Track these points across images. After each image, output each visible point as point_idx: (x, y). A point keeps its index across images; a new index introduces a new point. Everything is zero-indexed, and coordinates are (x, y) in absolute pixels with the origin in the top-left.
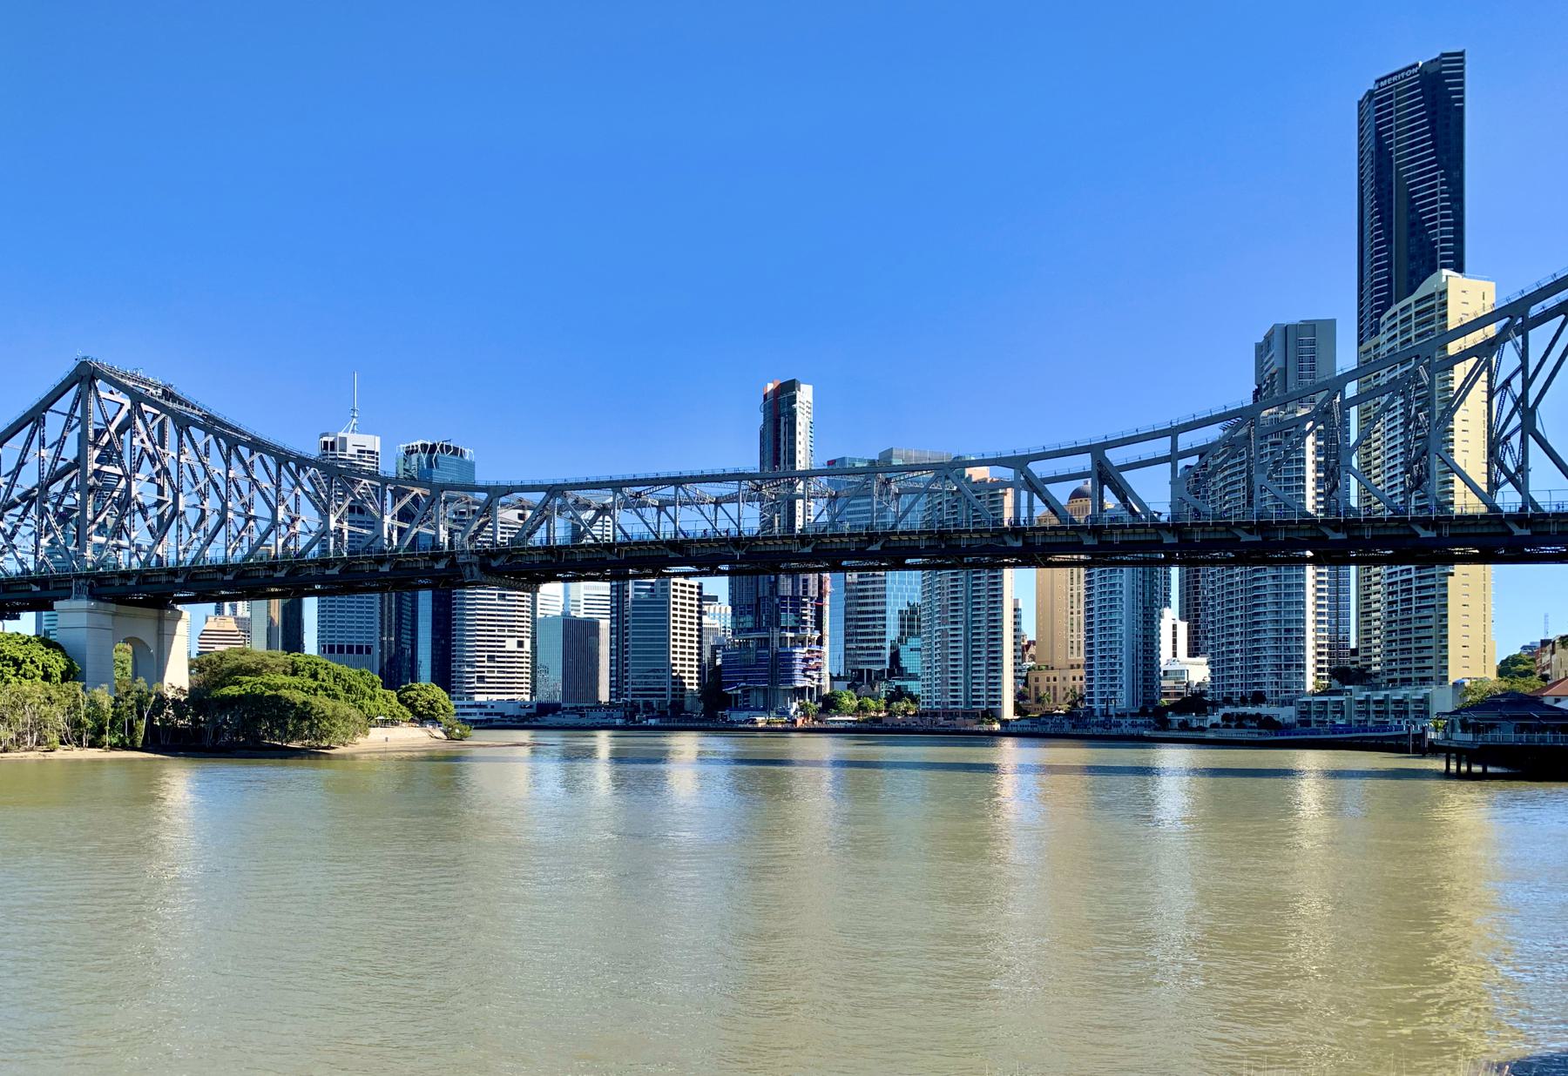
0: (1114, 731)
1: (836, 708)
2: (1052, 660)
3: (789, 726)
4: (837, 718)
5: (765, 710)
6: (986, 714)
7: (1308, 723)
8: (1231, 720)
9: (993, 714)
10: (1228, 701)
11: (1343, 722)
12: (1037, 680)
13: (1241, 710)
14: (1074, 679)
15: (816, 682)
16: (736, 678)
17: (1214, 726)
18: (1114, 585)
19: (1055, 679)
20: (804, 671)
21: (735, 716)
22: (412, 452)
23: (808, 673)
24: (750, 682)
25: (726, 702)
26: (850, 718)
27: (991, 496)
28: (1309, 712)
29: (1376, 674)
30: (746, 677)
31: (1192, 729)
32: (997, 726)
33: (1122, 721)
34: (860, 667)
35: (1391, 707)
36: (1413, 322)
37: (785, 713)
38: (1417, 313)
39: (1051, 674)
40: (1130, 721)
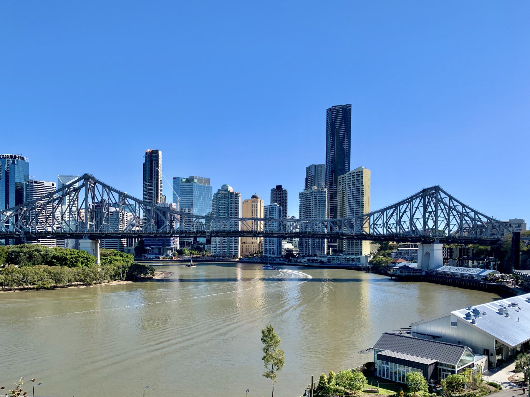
0: (274, 262)
1: (184, 254)
2: (247, 241)
3: (171, 259)
4: (185, 257)
5: (160, 254)
6: (234, 256)
7: (330, 262)
8: (310, 260)
9: (235, 256)
10: (308, 256)
11: (339, 262)
12: (243, 246)
13: (311, 258)
14: (254, 246)
15: (175, 246)
16: (150, 244)
17: (305, 262)
18: (273, 225)
19: (248, 246)
20: (173, 242)
21: (149, 256)
22: (5, 158)
23: (174, 243)
24: (156, 246)
25: (146, 251)
26: (189, 257)
27: (235, 197)
28: (330, 260)
29: (345, 251)
30: (154, 244)
31: (298, 262)
32: (238, 260)
33: (277, 259)
34: (184, 240)
35: (351, 260)
36: (355, 176)
37: (167, 255)
38: (356, 175)
39: (247, 245)
40: (279, 259)
